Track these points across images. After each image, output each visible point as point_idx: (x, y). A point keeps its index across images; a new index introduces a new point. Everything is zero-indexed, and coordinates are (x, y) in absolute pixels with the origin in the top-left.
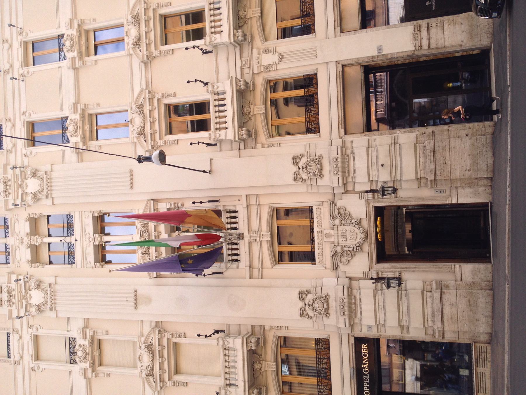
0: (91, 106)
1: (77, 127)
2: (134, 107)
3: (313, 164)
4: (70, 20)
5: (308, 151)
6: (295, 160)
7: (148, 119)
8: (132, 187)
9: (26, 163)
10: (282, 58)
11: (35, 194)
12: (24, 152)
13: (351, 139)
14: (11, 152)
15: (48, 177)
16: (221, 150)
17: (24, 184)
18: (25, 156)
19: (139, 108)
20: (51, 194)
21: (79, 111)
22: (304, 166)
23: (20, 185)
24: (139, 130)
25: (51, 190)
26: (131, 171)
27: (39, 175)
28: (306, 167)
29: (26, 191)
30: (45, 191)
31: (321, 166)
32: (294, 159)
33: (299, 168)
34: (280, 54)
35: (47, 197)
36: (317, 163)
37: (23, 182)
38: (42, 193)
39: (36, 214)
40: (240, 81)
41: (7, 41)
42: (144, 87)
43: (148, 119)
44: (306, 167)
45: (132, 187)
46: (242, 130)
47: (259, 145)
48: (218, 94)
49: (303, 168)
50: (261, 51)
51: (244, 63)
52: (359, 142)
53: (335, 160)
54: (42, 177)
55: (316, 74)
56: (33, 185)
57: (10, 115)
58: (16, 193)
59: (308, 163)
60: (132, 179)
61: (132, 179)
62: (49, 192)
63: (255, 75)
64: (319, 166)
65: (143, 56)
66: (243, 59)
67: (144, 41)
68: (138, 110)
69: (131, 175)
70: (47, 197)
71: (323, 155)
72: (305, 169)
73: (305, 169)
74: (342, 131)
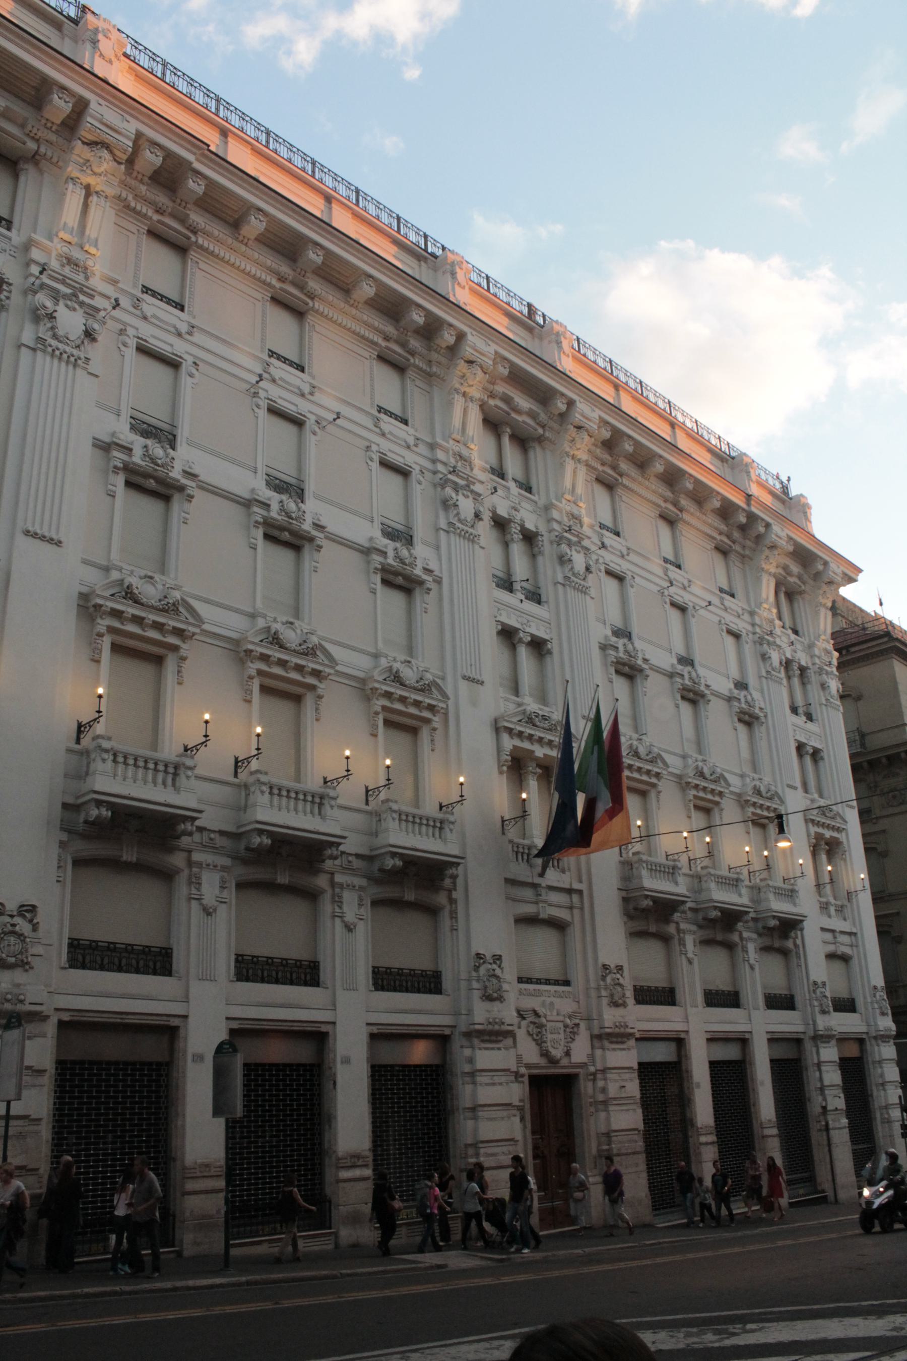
0: (186, 505)
1: (158, 465)
2: (177, 595)
3: (18, 947)
4: (323, 527)
5: (44, 941)
6: (28, 910)
7: (152, 617)
8: (27, 533)
9: (110, 323)
10: (208, 912)
11: (51, 317)
12: (131, 332)
13: (49, 1035)
14: (135, 307)
15: (79, 362)
16: (69, 751)
17: (77, 307)
18: (121, 330)
19: (174, 604)
20: (44, 351)
21: (184, 481)
22: (17, 928)
23: (76, 296)
24: (136, 591)
25: (53, 355)
26: (59, 543)
27: (86, 342)
28: (13, 933)
29: (61, 303)
30: (54, 343)
31: (11, 967)
32: (33, 909)
33: (12, 916)
34: (215, 910)
35: (39, 339)
36: (19, 956)
37: (82, 304)
38: (50, 333)
39: (8, 298)
40: (192, 825)
41: (312, 394)
42: (206, 627)
43: (152, 617)
44: (13, 933)
45: (27, 533)
46: (107, 810)
47: (64, 837)
48: (175, 775)
49: (14, 925)
50: (225, 874)
51: (212, 836)
52: (41, 1050)
53: (22, 997)
54: (82, 348)
55: (170, 974)
56: (71, 322)
57: (197, 337)
58: (61, 277)
59: (21, 936)
60: (43, 538)
61: (43, 538)
62: (50, 349)
63: (185, 854)
64: (13, 960)
65: (253, 643)
66: (217, 835)
67: (277, 654)
68: (171, 601)
69: (51, 541)
70: (39, 339)
71: (31, 972)
72: (11, 928)
73: (11, 928)
74: (66, 1017)
